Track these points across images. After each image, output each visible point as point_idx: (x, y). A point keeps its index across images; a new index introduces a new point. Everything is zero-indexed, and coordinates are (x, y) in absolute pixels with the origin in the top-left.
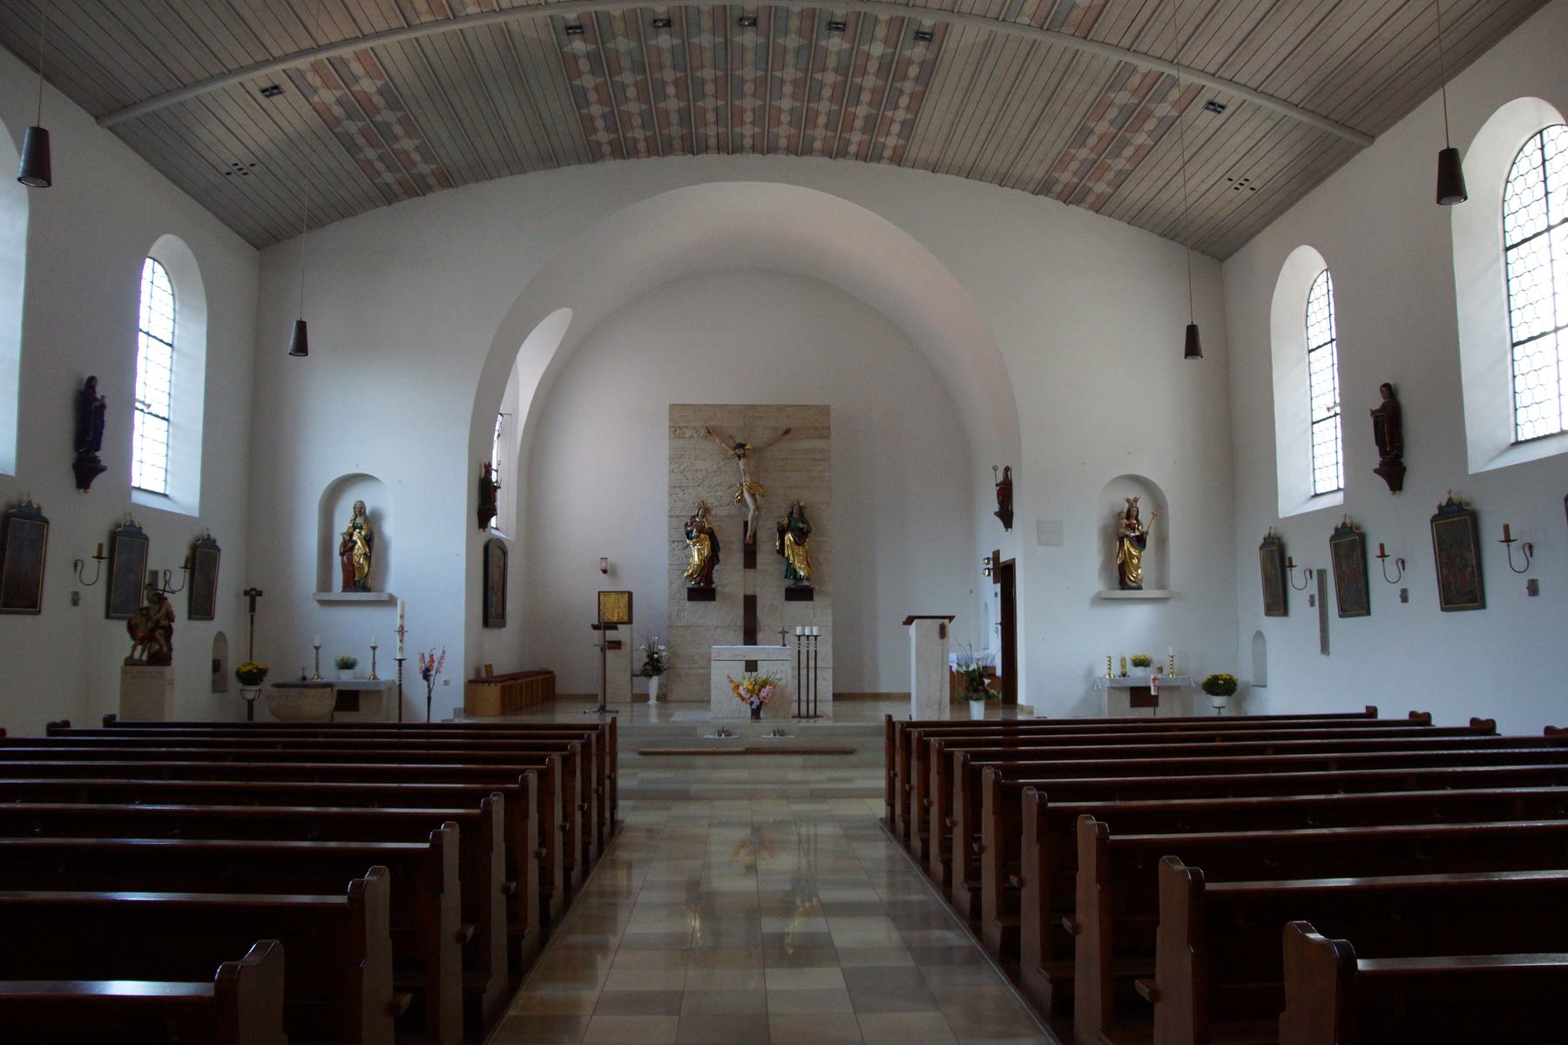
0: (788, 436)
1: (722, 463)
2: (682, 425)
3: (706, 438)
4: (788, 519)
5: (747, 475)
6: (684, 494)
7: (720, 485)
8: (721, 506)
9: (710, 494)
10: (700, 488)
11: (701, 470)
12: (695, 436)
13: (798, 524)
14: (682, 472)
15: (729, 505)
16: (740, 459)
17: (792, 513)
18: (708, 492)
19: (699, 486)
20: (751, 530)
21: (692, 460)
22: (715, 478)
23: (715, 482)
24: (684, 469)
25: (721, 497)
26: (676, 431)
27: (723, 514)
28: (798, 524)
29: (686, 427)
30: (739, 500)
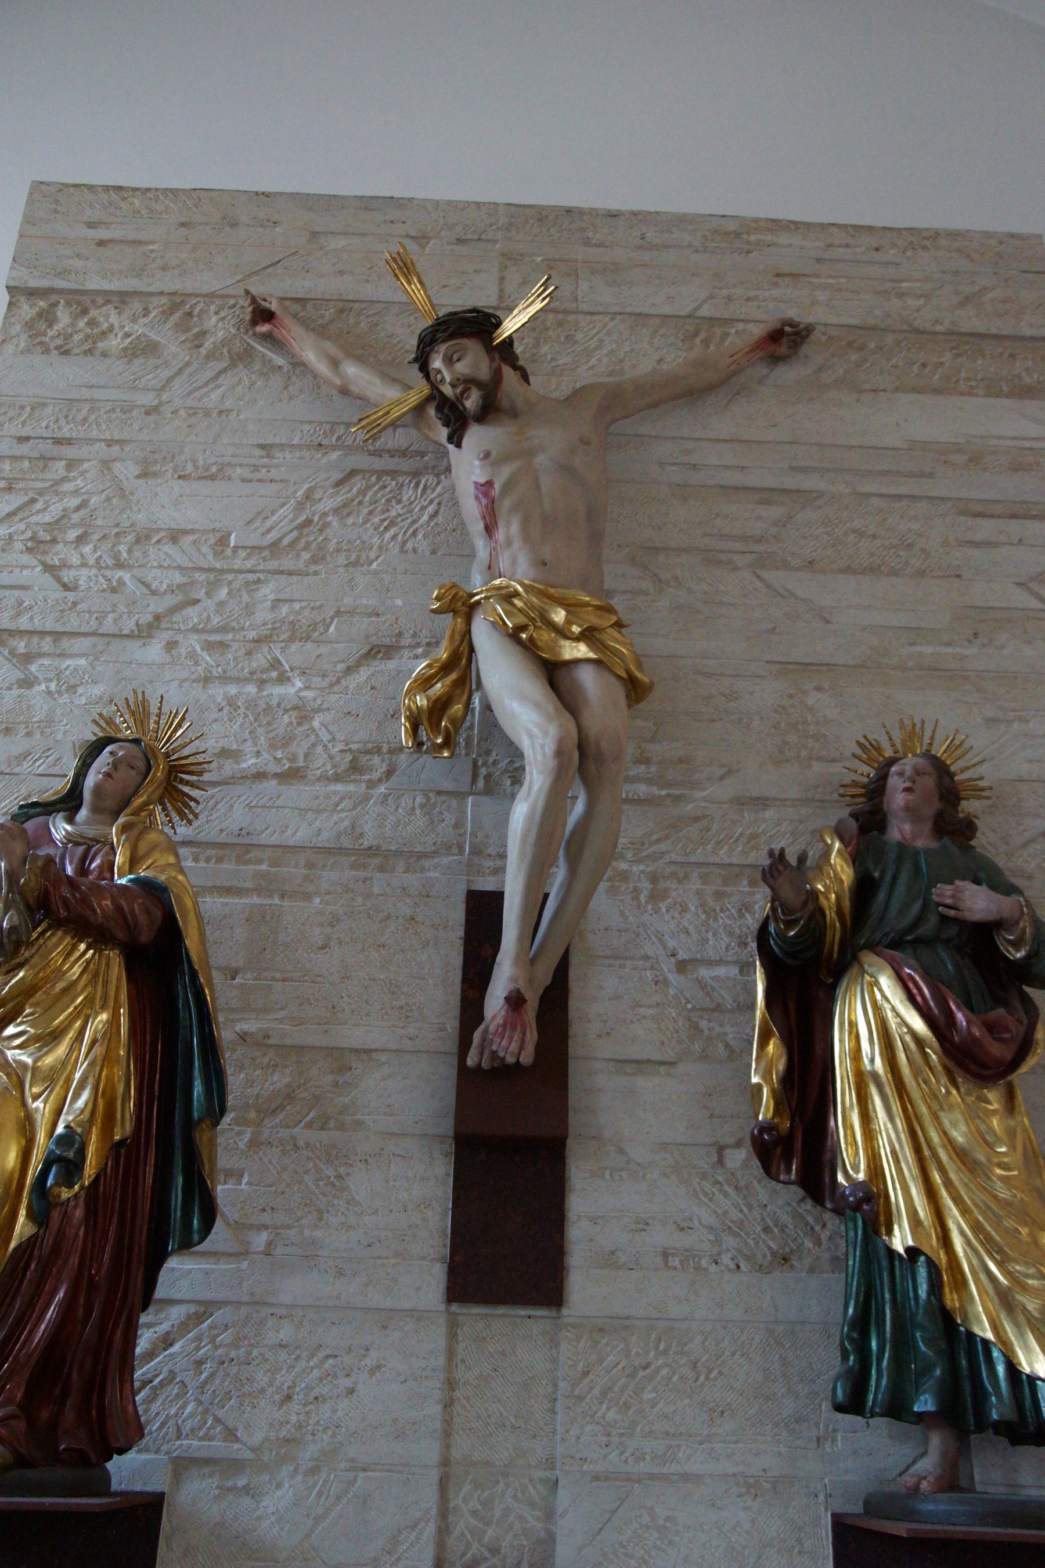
0: (788, 374)
1: (328, 504)
2: (95, 283)
3: (243, 357)
4: (856, 859)
5: (510, 528)
6: (27, 683)
7: (299, 634)
8: (292, 775)
9: (219, 692)
10: (154, 651)
11: (175, 536)
12: (173, 346)
13: (944, 892)
14: (36, 546)
15: (355, 768)
16: (456, 439)
17: (877, 789)
18: (206, 680)
19: (144, 633)
20: (529, 961)
21: (127, 470)
22: (267, 592)
23: (262, 615)
24: (58, 524)
25: (303, 712)
26: (48, 317)
27: (301, 833)
28: (944, 892)
29: (122, 298)
30: (439, 707)
